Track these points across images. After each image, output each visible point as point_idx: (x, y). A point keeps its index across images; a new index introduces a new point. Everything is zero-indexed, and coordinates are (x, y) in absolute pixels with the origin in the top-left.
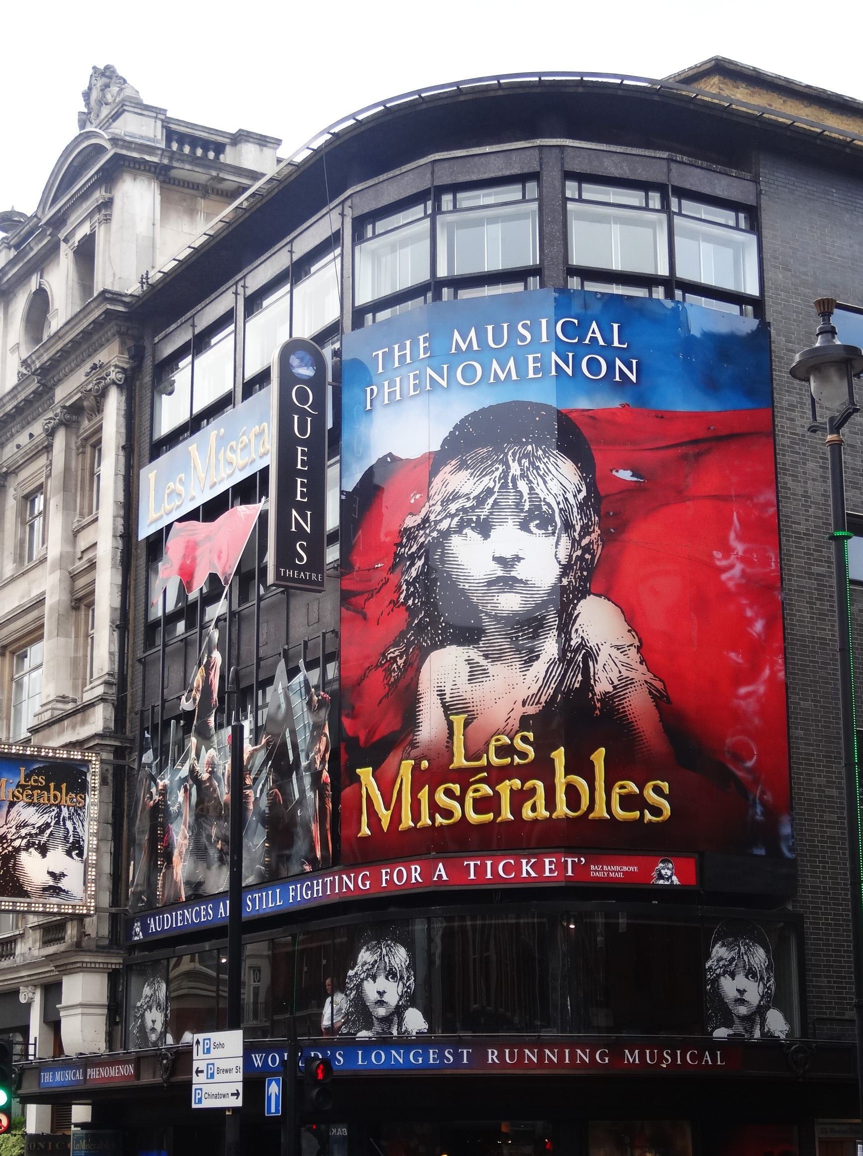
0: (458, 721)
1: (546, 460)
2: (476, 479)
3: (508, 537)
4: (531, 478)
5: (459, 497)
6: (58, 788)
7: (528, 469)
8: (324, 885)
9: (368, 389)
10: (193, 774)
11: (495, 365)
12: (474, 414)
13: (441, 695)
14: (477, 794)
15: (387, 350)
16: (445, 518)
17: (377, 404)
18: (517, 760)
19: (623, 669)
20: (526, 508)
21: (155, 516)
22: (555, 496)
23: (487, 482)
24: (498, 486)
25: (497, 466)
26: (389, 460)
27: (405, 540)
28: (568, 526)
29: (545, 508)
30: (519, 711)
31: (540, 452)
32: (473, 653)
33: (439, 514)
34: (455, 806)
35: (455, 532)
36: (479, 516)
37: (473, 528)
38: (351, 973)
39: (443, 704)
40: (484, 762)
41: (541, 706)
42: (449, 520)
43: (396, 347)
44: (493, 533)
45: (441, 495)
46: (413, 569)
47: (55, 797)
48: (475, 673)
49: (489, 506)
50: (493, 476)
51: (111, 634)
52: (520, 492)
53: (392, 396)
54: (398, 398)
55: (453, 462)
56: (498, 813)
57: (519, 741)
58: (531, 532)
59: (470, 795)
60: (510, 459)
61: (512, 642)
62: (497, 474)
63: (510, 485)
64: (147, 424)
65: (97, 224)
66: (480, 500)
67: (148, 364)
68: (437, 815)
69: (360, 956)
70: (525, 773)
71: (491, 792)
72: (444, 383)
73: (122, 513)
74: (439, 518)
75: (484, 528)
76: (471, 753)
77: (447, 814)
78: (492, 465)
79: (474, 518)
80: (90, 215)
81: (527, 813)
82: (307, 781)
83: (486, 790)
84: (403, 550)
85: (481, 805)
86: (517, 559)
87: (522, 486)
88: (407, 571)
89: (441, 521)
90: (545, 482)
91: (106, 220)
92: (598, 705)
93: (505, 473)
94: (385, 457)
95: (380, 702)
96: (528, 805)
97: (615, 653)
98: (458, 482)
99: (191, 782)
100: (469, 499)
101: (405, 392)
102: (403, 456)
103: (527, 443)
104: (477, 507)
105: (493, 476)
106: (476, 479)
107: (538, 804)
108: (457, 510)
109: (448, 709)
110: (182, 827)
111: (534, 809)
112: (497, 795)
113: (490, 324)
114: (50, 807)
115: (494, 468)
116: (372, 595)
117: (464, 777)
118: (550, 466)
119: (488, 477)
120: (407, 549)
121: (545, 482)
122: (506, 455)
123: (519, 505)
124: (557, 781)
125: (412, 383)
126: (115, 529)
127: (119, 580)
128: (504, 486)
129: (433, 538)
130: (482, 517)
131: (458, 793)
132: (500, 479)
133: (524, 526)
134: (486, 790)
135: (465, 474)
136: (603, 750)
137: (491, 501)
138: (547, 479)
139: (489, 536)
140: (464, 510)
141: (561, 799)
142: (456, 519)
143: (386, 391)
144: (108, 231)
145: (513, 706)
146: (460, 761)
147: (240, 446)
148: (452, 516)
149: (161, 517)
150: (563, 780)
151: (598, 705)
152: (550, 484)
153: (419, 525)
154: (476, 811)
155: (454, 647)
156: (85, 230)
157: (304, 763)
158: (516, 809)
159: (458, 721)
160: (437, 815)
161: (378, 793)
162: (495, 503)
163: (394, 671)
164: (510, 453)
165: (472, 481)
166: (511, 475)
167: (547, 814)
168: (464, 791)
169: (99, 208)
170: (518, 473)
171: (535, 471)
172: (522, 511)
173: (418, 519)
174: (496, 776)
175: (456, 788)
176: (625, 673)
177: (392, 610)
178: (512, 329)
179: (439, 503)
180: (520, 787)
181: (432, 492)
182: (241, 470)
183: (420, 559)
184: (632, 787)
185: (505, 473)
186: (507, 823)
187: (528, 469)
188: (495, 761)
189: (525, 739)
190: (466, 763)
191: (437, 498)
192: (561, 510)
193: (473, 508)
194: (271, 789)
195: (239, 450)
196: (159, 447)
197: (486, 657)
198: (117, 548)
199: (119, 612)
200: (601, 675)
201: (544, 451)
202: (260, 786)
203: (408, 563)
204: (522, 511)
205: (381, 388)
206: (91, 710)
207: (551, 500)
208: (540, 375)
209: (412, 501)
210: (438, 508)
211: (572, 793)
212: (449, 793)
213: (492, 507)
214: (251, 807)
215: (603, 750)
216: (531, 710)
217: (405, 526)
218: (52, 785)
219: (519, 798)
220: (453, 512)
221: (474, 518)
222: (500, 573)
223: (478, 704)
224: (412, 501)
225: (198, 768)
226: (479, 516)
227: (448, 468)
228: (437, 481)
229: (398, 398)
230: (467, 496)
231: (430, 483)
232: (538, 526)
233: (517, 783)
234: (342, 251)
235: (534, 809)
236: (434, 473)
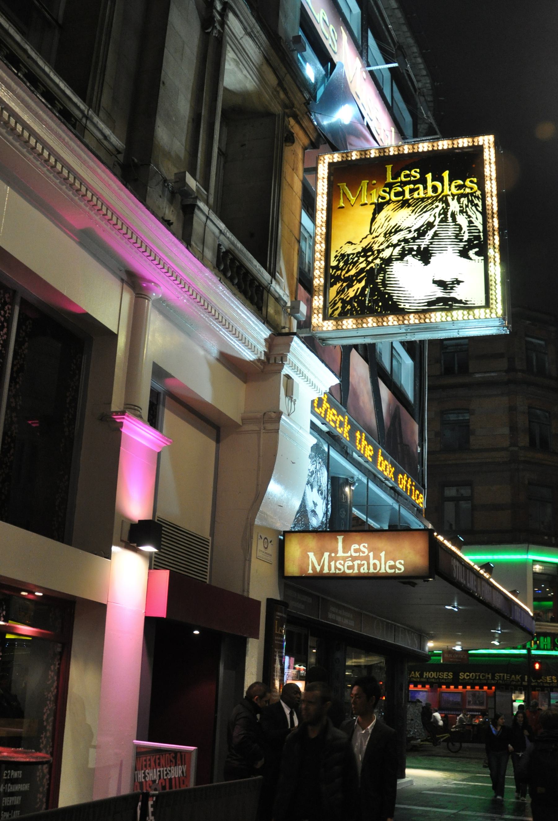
2: (417, 215)
3: (448, 262)
4: (470, 213)
5: (401, 230)
7: (467, 206)
16: (388, 247)
20: (466, 237)
24: (438, 220)
25: (437, 204)
33: (382, 244)
35: (397, 259)
42: (391, 249)
44: (432, 260)
45: (384, 228)
49: (430, 237)
50: (433, 213)
52: (459, 225)
58: (469, 258)
62: (437, 211)
63: (450, 219)
78: (432, 203)
79: (415, 248)
89: (383, 250)
100: (410, 231)
104: (418, 238)
105: (433, 213)
106: (417, 215)
115: (434, 206)
119: (428, 213)
128: (444, 220)
130: (422, 247)
132: (440, 215)
133: (464, 254)
137: (431, 233)
139: (429, 262)
142: (398, 248)
148: (395, 246)
162: (436, 234)
165: (413, 216)
171: (474, 208)
179: (382, 235)
187: (467, 206)
193: (414, 239)
204: (461, 241)
210: (381, 239)
213: (432, 238)
220: (395, 242)
221: (415, 248)
222: (439, 293)
226: (419, 245)
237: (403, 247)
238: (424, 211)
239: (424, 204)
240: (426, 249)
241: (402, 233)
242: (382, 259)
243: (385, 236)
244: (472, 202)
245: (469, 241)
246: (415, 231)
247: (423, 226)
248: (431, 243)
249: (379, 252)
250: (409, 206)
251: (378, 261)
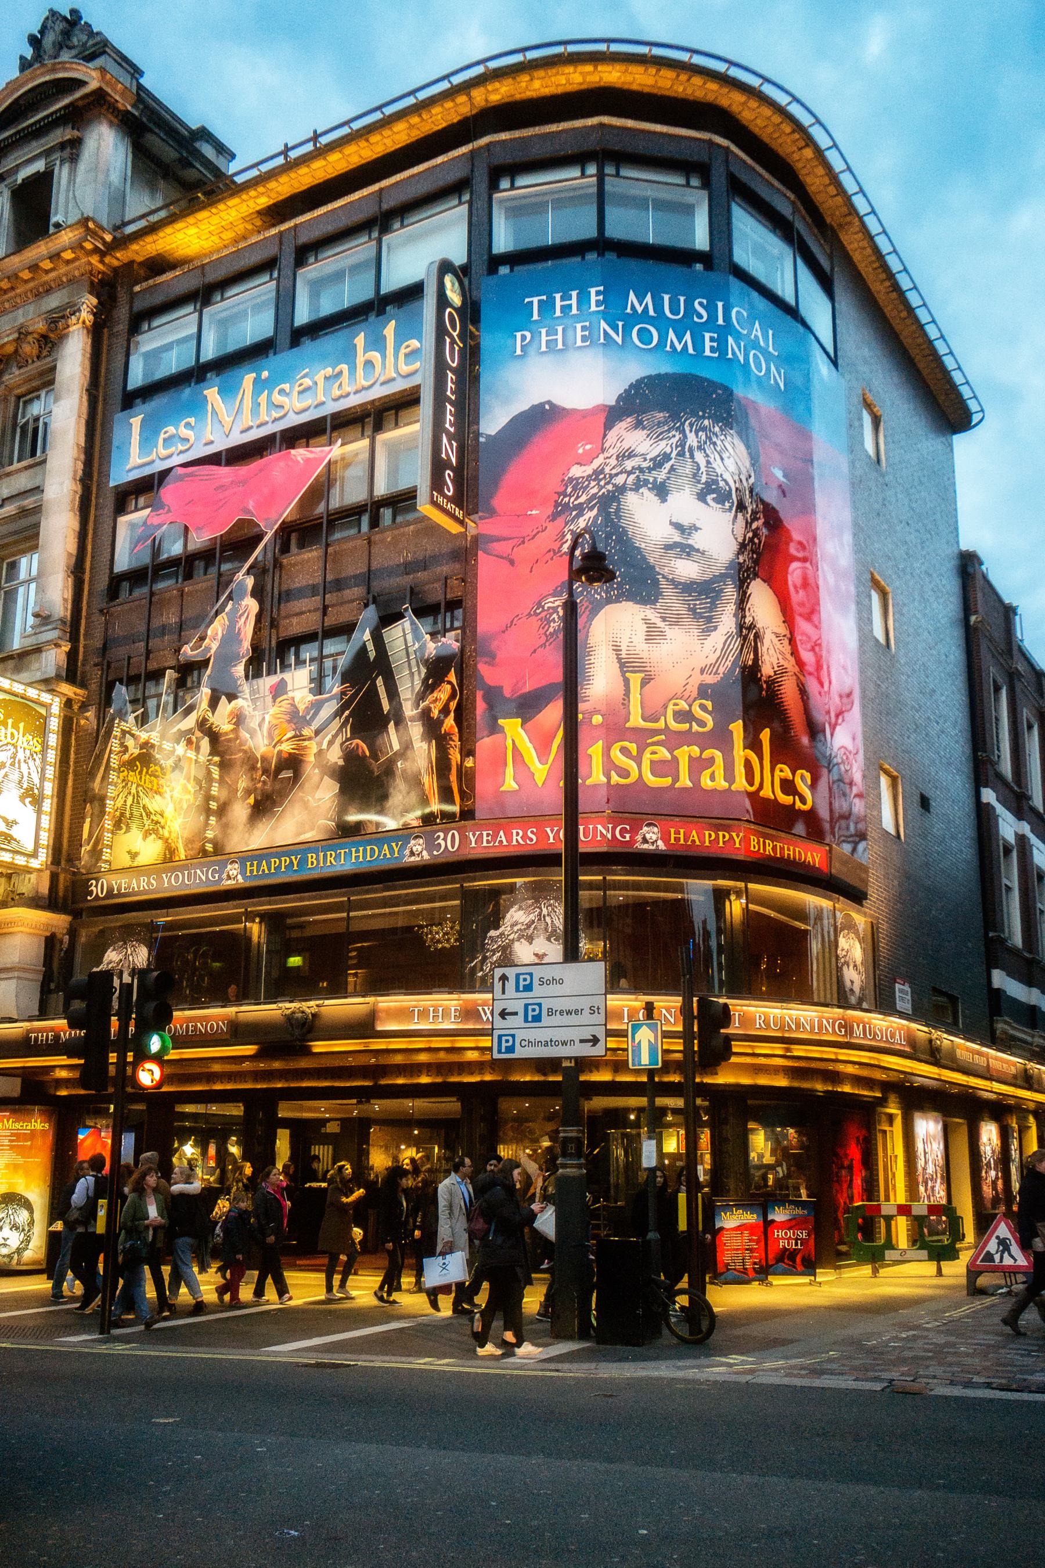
0: (635, 679)
1: (723, 437)
2: (652, 441)
3: (683, 504)
5: (636, 456)
6: (15, 726)
8: (365, 850)
9: (519, 335)
10: (203, 725)
11: (671, 335)
12: (649, 377)
13: (617, 650)
14: (655, 757)
15: (544, 297)
16: (621, 472)
17: (532, 350)
18: (695, 727)
19: (780, 657)
20: (703, 480)
21: (139, 461)
22: (732, 474)
23: (663, 446)
25: (674, 433)
26: (547, 407)
27: (569, 490)
29: (722, 484)
30: (697, 680)
31: (717, 429)
32: (650, 613)
35: (631, 490)
36: (655, 478)
37: (649, 489)
38: (493, 933)
39: (619, 660)
40: (661, 725)
41: (718, 678)
42: (625, 476)
43: (558, 296)
44: (669, 498)
46: (581, 520)
47: (12, 735)
48: (653, 634)
49: (666, 471)
50: (670, 442)
51: (66, 580)
53: (552, 345)
54: (560, 346)
55: (629, 420)
56: (676, 779)
57: (698, 709)
59: (647, 756)
60: (687, 429)
61: (689, 609)
62: (674, 440)
63: (687, 454)
64: (120, 372)
65: (58, 162)
66: (658, 463)
67: (122, 313)
68: (613, 773)
69: (508, 916)
70: (705, 741)
71: (668, 756)
72: (619, 340)
73: (82, 457)
74: (614, 472)
75: (662, 491)
76: (648, 713)
78: (669, 431)
80: (47, 153)
81: (706, 782)
82: (416, 730)
83: (664, 753)
84: (567, 499)
86: (697, 529)
88: (573, 520)
89: (617, 475)
90: (722, 459)
91: (72, 159)
92: (765, 686)
93: (682, 443)
94: (542, 405)
95: (535, 651)
96: (708, 772)
97: (775, 640)
98: (637, 441)
99: (199, 734)
100: (645, 460)
101: (570, 341)
102: (568, 405)
103: (704, 417)
104: (654, 469)
106: (652, 441)
107: (716, 774)
108: (633, 468)
109: (625, 666)
110: (182, 781)
111: (712, 778)
112: (675, 760)
113: (667, 293)
114: (7, 745)
115: (670, 435)
116: (523, 542)
117: (642, 737)
118: (727, 444)
119: (664, 442)
120: (572, 499)
121: (722, 459)
122: (683, 424)
124: (735, 752)
125: (579, 333)
126: (75, 472)
127: (76, 525)
128: (681, 454)
129: (608, 491)
131: (635, 753)
132: (677, 447)
133: (702, 497)
134: (664, 753)
135: (640, 434)
136: (768, 730)
137: (668, 466)
138: (724, 456)
140: (641, 470)
141: (740, 773)
142: (632, 477)
143: (544, 338)
144: (73, 172)
145: (691, 673)
146: (636, 720)
147: (297, 389)
148: (629, 473)
149: (170, 456)
150: (742, 753)
151: (765, 686)
152: (726, 461)
153: (589, 476)
154: (654, 773)
155: (631, 603)
156: (40, 166)
157: (409, 710)
159: (635, 679)
160: (613, 773)
161: (530, 746)
162: (672, 469)
163: (554, 620)
164: (687, 423)
165: (648, 442)
166: (687, 445)
167: (726, 785)
168: (641, 751)
169: (62, 146)
170: (695, 444)
172: (699, 482)
173: (589, 470)
174: (675, 739)
175: (633, 747)
176: (782, 662)
177: (552, 559)
178: (689, 305)
179: (614, 457)
180: (698, 754)
181: (607, 445)
182: (297, 413)
183: (591, 509)
184: (787, 773)
185: (682, 443)
186: (685, 789)
187: (705, 443)
189: (703, 708)
190: (643, 724)
191: (612, 451)
192: (737, 489)
194: (347, 740)
195: (295, 394)
196: (130, 399)
197: (664, 619)
198: (76, 492)
199: (74, 559)
200: (766, 657)
201: (722, 430)
202: (329, 737)
203: (574, 513)
204: (699, 482)
205: (536, 335)
206: (33, 657)
207: (727, 476)
208: (716, 355)
209: (581, 451)
210: (613, 462)
212: (624, 751)
213: (669, 473)
214: (311, 759)
215: (768, 730)
216: (710, 679)
217: (570, 475)
218: (10, 721)
219: (698, 766)
220: (629, 468)
222: (677, 538)
223: (655, 664)
224: (581, 451)
225: (211, 720)
226: (655, 478)
227: (623, 424)
228: (612, 435)
229: (560, 346)
230: (643, 456)
231: (605, 436)
232: (713, 499)
233: (695, 750)
234: (471, 198)
235: (712, 778)
236: (609, 426)
237: (638, 477)
238: (659, 438)
239: (660, 430)
240: (663, 484)
241: (637, 459)
242: (614, 485)
243: (617, 459)
244: (710, 439)
245: (706, 483)
246: (651, 460)
247: (658, 456)
248: (668, 478)
249: (611, 476)
250: (644, 428)
251: (610, 487)
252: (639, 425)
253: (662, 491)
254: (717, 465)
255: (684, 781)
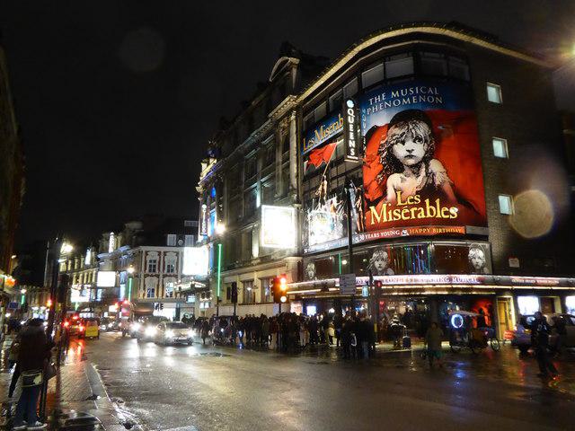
0: (399, 193)
3: (410, 144)
23: (403, 130)
28: (426, 141)
32: (402, 175)
34: (399, 215)
48: (403, 180)
66: (402, 136)
75: (403, 143)
77: (397, 217)
81: (419, 217)
83: (407, 211)
85: (406, 215)
87: (413, 131)
98: (397, 131)
123: (412, 136)
133: (414, 142)
146: (400, 203)
158: (416, 215)
159: (399, 193)
174: (410, 207)
175: (399, 211)
188: (409, 203)
211: (431, 210)
233: (416, 209)
252: (396, 127)
253: (403, 143)
254: (418, 132)
255: (413, 217)
